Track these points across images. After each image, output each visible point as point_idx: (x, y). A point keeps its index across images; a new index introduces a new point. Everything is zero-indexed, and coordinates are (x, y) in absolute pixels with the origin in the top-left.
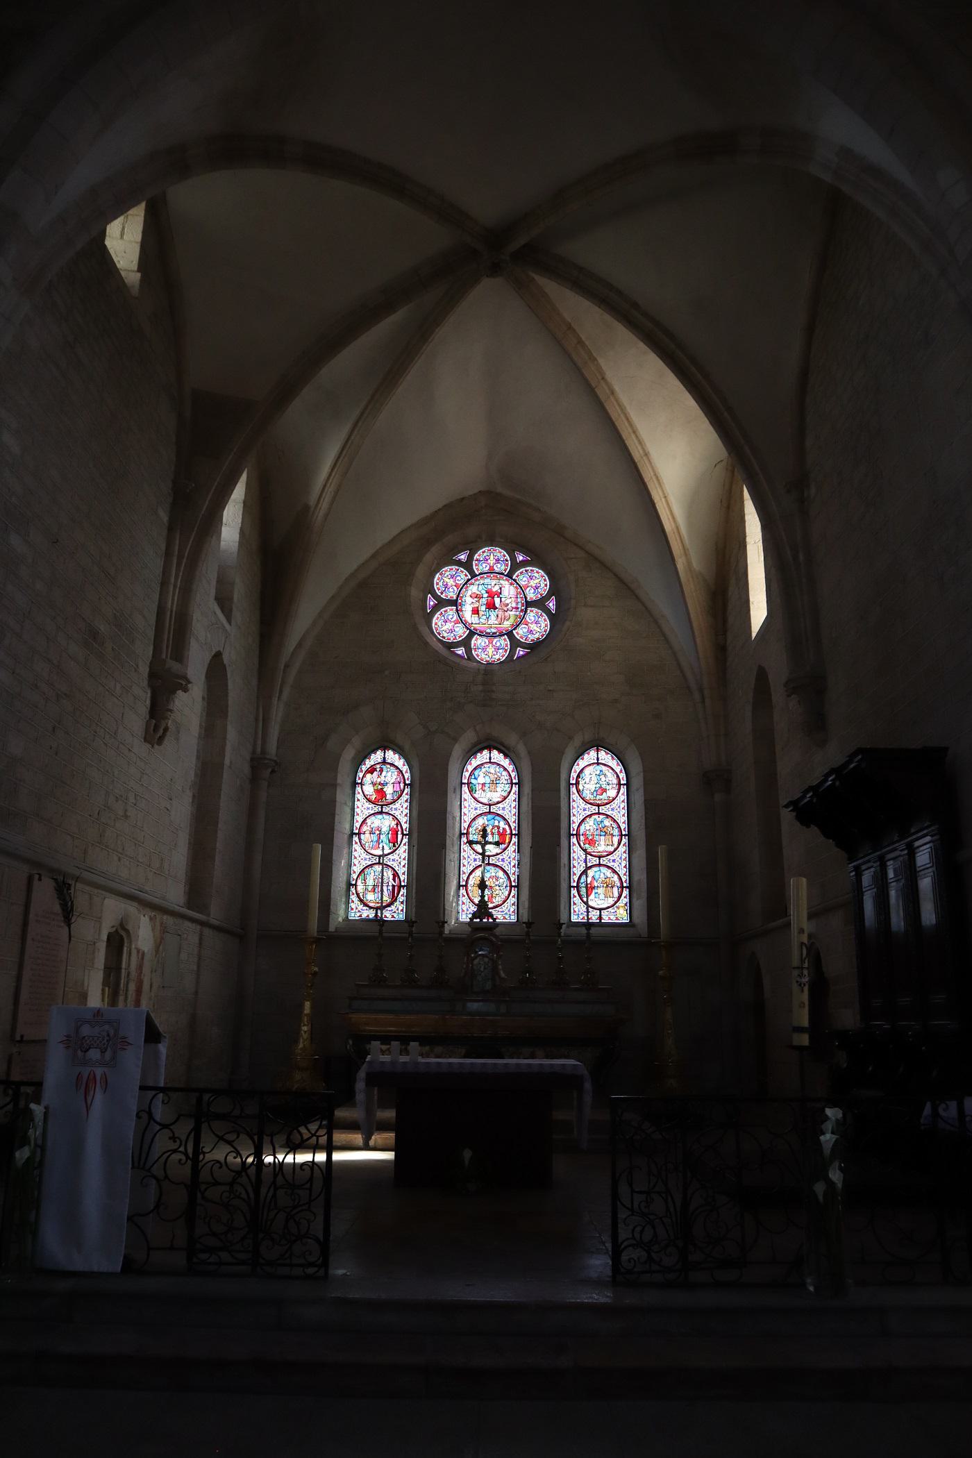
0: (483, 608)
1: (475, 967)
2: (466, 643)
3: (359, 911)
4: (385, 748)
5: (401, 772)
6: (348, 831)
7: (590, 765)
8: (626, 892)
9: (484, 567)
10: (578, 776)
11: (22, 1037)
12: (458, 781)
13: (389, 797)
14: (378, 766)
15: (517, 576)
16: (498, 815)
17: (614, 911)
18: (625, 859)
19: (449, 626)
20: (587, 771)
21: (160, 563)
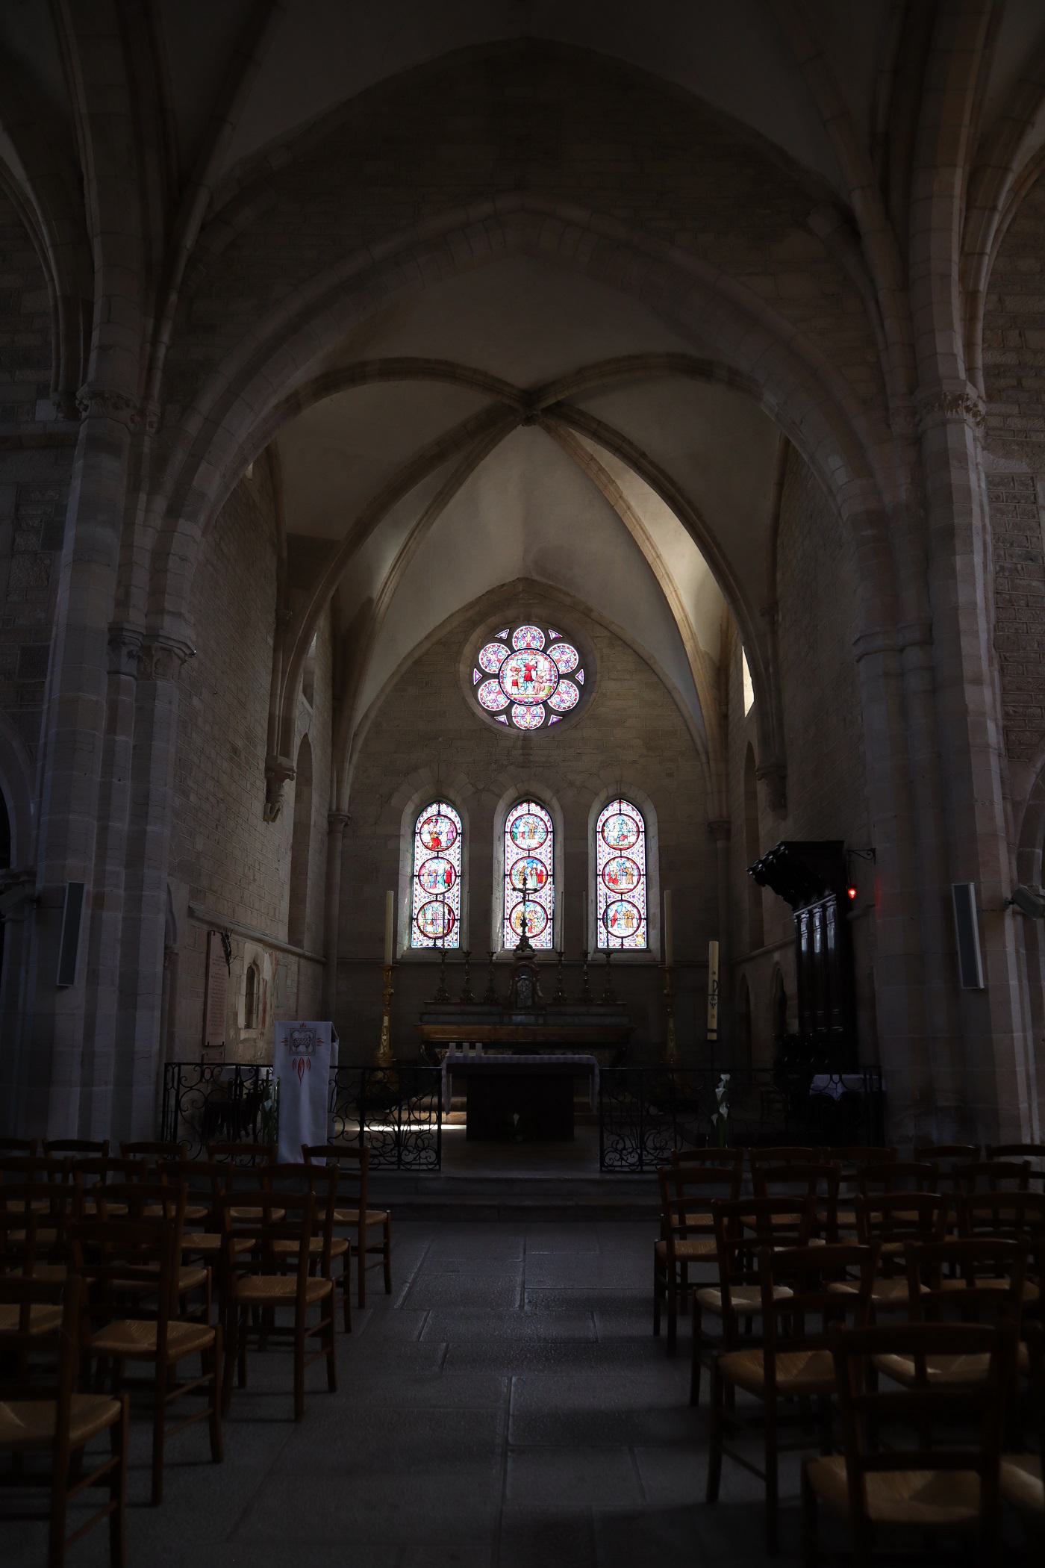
0: (521, 680)
1: (519, 988)
2: (507, 711)
4: (439, 802)
5: (454, 822)
6: (409, 874)
7: (613, 815)
8: (644, 923)
9: (522, 644)
10: (604, 825)
11: (208, 1043)
12: (502, 831)
13: (444, 844)
14: (434, 818)
15: (551, 652)
16: (536, 859)
19: (492, 696)
20: (610, 820)
21: (269, 678)
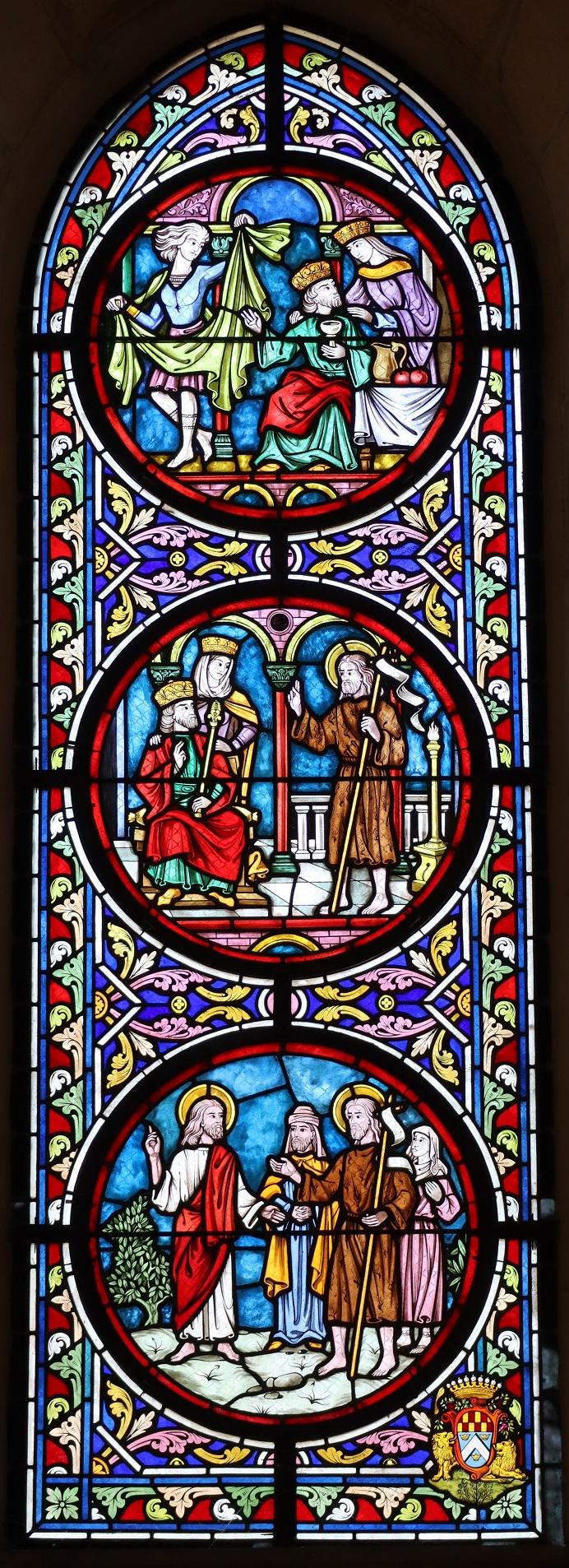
17: (402, 1441)
18: (503, 990)
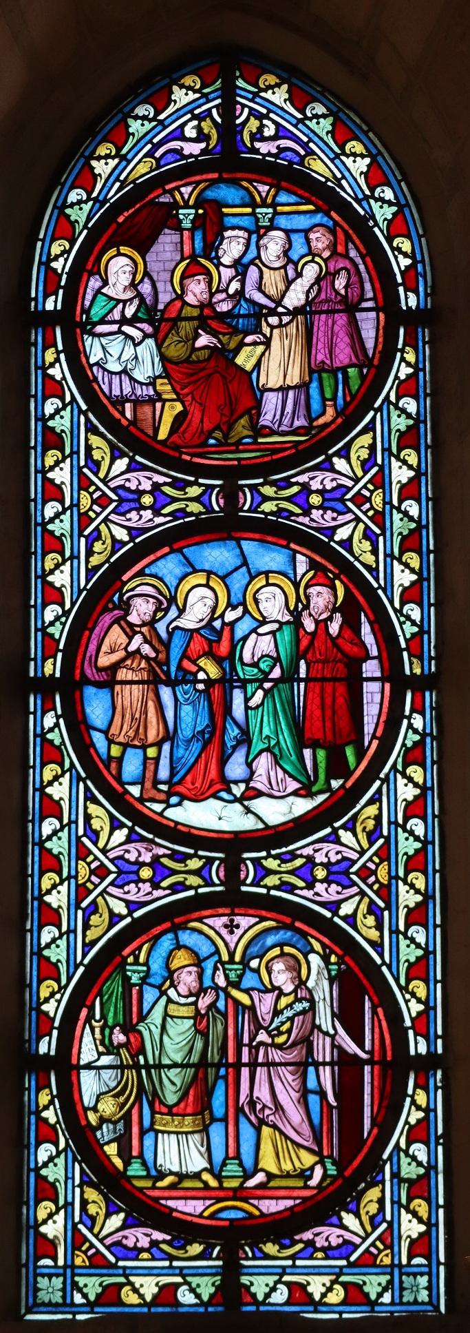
3: (97, 1262)
5: (361, 226)
